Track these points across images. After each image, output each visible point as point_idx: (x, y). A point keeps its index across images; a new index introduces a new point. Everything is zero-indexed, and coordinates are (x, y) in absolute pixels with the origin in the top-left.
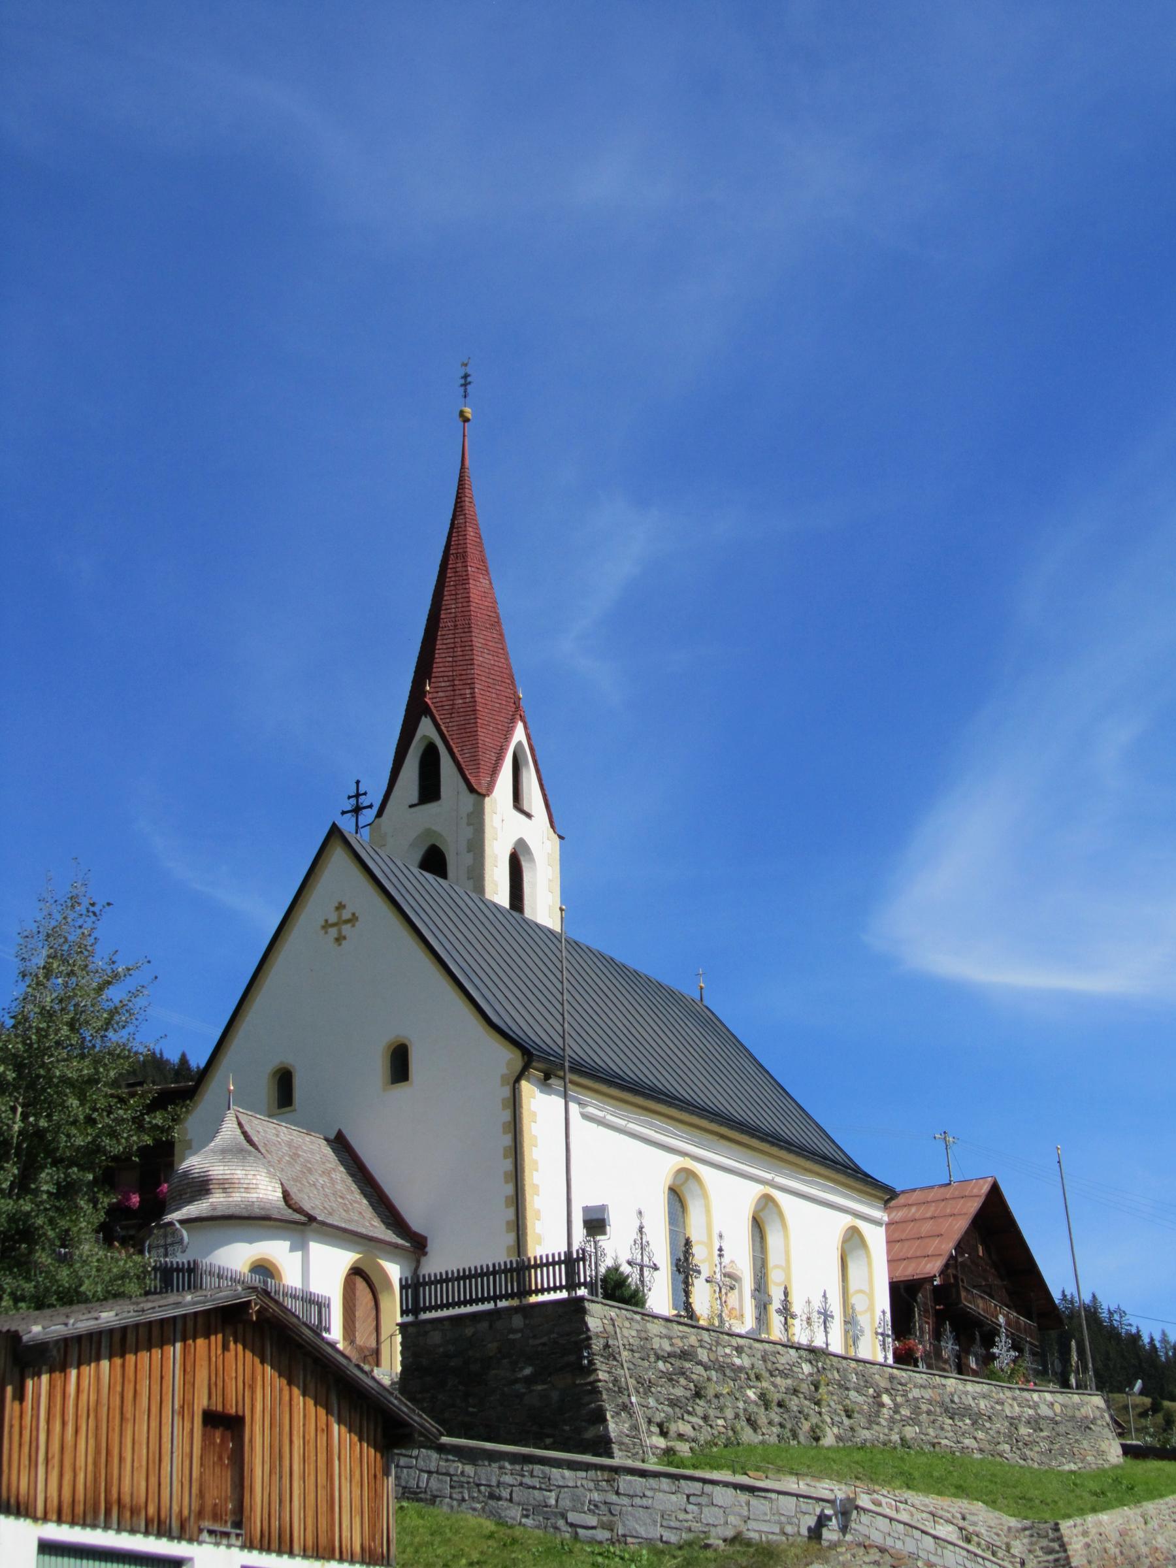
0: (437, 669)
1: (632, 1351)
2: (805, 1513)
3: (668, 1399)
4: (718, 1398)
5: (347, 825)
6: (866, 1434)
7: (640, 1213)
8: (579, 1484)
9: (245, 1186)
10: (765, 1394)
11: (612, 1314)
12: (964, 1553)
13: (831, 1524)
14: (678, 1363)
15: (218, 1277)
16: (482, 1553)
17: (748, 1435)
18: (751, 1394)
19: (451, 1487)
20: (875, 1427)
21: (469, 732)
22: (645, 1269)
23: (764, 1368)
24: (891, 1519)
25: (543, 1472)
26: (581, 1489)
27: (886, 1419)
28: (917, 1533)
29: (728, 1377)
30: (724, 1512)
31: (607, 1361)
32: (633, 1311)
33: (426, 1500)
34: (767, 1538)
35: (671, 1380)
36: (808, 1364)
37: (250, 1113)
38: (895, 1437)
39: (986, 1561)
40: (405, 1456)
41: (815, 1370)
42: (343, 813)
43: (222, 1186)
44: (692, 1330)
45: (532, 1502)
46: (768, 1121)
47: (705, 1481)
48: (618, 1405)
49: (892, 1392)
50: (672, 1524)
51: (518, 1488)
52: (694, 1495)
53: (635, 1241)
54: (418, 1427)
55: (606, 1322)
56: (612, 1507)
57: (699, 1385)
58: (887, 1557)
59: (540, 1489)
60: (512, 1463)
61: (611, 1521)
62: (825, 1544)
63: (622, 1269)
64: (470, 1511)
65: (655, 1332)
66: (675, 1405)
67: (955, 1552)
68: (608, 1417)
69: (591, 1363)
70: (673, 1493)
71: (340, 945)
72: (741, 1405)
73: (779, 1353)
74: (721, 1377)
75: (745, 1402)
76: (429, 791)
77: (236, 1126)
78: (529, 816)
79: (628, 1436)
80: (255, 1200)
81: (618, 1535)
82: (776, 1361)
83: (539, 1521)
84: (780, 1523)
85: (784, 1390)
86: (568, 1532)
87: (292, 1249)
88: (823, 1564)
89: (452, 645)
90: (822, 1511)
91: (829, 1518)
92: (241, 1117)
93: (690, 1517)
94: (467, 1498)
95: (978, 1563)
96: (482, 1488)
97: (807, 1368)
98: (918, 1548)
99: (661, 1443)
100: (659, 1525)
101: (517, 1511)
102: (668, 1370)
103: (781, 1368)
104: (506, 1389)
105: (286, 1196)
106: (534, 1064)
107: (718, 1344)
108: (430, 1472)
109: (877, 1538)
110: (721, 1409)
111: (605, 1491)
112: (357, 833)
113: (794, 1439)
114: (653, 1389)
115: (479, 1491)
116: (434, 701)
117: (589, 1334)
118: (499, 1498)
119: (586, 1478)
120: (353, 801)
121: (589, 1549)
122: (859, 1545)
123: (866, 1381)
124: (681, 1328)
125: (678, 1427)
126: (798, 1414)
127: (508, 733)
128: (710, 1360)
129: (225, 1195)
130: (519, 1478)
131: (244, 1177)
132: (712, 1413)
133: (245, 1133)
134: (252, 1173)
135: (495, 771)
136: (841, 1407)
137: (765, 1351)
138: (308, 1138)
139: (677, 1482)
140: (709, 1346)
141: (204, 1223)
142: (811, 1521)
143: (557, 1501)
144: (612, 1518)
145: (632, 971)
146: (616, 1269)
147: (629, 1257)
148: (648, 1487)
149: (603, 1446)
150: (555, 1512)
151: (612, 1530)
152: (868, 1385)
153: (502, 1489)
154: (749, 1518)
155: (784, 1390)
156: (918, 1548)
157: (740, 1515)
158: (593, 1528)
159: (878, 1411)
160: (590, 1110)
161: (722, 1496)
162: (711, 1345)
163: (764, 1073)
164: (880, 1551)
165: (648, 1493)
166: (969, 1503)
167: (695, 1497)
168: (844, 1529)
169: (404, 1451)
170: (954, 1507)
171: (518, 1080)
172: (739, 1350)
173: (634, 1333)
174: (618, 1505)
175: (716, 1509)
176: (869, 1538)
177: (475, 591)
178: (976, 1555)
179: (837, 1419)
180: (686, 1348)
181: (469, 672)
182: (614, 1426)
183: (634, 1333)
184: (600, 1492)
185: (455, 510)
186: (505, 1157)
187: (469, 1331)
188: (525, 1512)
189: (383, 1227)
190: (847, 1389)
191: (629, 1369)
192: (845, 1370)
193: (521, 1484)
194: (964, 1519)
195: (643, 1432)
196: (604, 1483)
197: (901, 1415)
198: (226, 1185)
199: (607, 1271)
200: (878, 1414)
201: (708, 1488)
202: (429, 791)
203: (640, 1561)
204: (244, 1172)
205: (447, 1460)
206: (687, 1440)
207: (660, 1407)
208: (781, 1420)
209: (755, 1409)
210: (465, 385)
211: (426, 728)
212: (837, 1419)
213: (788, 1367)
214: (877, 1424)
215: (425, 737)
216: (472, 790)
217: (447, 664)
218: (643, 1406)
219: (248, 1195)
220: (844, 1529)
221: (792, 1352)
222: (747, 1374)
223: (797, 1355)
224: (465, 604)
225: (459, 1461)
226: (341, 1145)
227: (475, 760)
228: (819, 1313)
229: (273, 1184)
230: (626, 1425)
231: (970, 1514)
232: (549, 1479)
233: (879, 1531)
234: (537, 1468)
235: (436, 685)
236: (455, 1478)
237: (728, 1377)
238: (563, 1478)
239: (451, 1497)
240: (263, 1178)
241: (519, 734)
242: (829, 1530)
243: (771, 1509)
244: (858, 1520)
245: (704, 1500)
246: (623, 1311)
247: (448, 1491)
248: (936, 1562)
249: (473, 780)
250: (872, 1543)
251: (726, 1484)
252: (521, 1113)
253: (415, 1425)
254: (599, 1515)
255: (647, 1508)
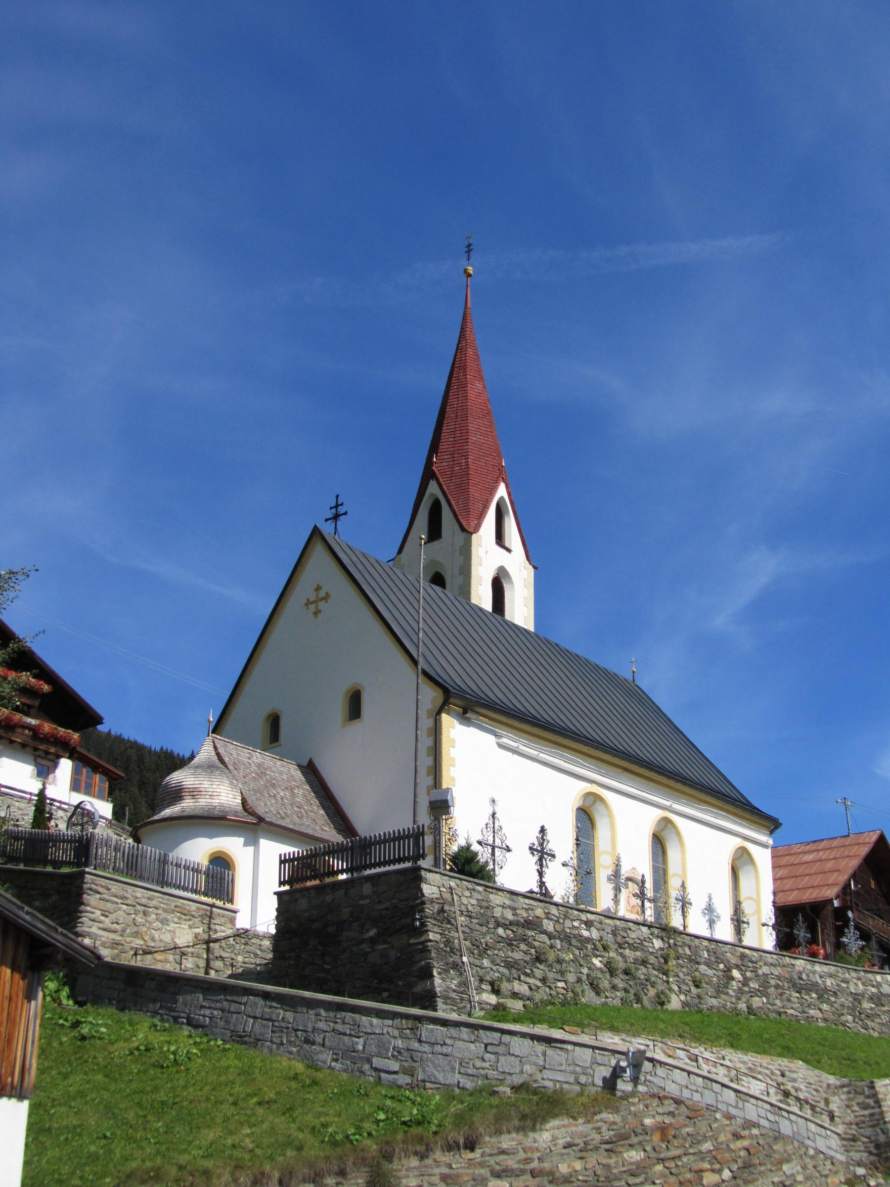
0: (442, 447)
1: (470, 917)
2: (600, 1064)
3: (505, 961)
4: (561, 963)
5: (327, 529)
6: (714, 1002)
7: (494, 801)
8: (385, 1031)
9: (210, 793)
10: (611, 962)
11: (451, 883)
12: (768, 1107)
13: (626, 1075)
14: (520, 931)
15: (184, 868)
16: (278, 1093)
17: (589, 997)
18: (596, 962)
19: (273, 1032)
20: (723, 996)
21: (463, 489)
22: (496, 849)
23: (613, 941)
24: (689, 1073)
25: (354, 1020)
26: (387, 1036)
27: (734, 990)
28: (717, 1087)
29: (574, 946)
30: (520, 1061)
31: (440, 924)
32: (475, 883)
33: (250, 1043)
34: (561, 1086)
35: (510, 945)
36: (660, 940)
37: (227, 740)
38: (742, 1006)
39: (791, 1115)
40: (236, 1002)
41: (667, 945)
42: (327, 520)
43: (191, 794)
44: (539, 904)
45: (342, 1046)
46: (672, 762)
47: (503, 1032)
48: (447, 964)
49: (743, 968)
50: (470, 1071)
51: (330, 1034)
52: (492, 1044)
53: (487, 825)
54: (63, 947)
55: (444, 890)
56: (414, 1053)
57: (539, 950)
58: (683, 1108)
59: (350, 1035)
60: (327, 1010)
61: (412, 1067)
62: (619, 1094)
63: (473, 848)
64: (287, 1054)
65: (497, 902)
66: (512, 967)
67: (757, 1106)
68: (435, 973)
69: (423, 924)
70: (472, 1042)
71: (317, 617)
72: (585, 971)
73: (630, 929)
74: (566, 945)
75: (589, 968)
76: (434, 533)
77: (212, 749)
78: (509, 550)
79: (454, 991)
80: (217, 804)
81: (418, 1081)
82: (626, 935)
83: (347, 1065)
84: (574, 1072)
85: (632, 961)
86: (372, 1076)
87: (246, 844)
88: (612, 1114)
89: (454, 430)
90: (618, 1062)
91: (623, 1070)
92: (216, 741)
93: (486, 1065)
94: (285, 1042)
95: (782, 1116)
96: (299, 1033)
97: (658, 943)
98: (717, 1101)
99: (493, 999)
100: (457, 1072)
101: (328, 1055)
102: (507, 935)
103: (631, 942)
104: (354, 948)
105: (244, 802)
106: (452, 700)
107: (566, 917)
108: (255, 1018)
109: (672, 1089)
110: (562, 973)
111: (409, 1038)
112: (335, 534)
113: (637, 1003)
114: (489, 952)
115: (296, 1036)
116: (439, 468)
117: (424, 899)
118: (313, 1043)
119: (392, 1026)
120: (334, 511)
121: (383, 1092)
122: (653, 1096)
123: (718, 958)
124: (527, 901)
125: (513, 986)
126: (644, 981)
127: (493, 490)
128: (556, 930)
129: (193, 800)
130: (332, 1024)
131: (210, 786)
132: (551, 975)
133: (218, 754)
134: (217, 783)
135: (481, 516)
136: (690, 978)
137: (616, 926)
138: (279, 763)
139: (476, 1032)
140: (556, 919)
141: (174, 822)
142: (606, 1072)
143: (364, 1047)
144: (413, 1064)
145: (584, 660)
146: (468, 848)
147: (480, 838)
148: (449, 1036)
149: (428, 1000)
150: (362, 1057)
151: (413, 1076)
152: (719, 961)
153: (316, 1034)
154: (544, 1068)
155: (632, 961)
156: (717, 1101)
157: (536, 1065)
158: (395, 1073)
159: (728, 983)
160: (504, 740)
161: (519, 1046)
162: (558, 918)
163: (679, 734)
164: (676, 1103)
165: (448, 1041)
166: (789, 1062)
167: (493, 1047)
168: (635, 1080)
169: (235, 998)
170: (773, 1064)
171: (439, 713)
172: (589, 924)
173: (474, 902)
174: (420, 1052)
175: (513, 1058)
176: (665, 1090)
177: (471, 392)
178: (780, 1109)
179: (684, 987)
180: (531, 918)
181: (464, 447)
182: (440, 981)
183: (474, 902)
184: (404, 1040)
185: (460, 338)
186: (428, 775)
187: (329, 898)
188: (335, 1057)
189: (334, 832)
190: (698, 963)
191: (463, 932)
192: (696, 947)
193: (333, 1030)
194: (783, 1075)
195: (472, 989)
196: (408, 1031)
197: (750, 987)
198: (195, 793)
199: (459, 850)
200: (726, 986)
201: (506, 1038)
202: (434, 533)
203: (427, 1106)
204: (210, 783)
205: (271, 1007)
206: (520, 999)
207: (494, 968)
208: (626, 986)
209: (599, 975)
210: (468, 252)
211: (433, 488)
212: (684, 987)
213: (638, 941)
214: (725, 994)
215: (432, 494)
216: (463, 529)
217: (449, 443)
218: (476, 966)
219: (212, 801)
220: (635, 1080)
221: (645, 929)
222: (594, 944)
223: (649, 932)
224: (465, 401)
225: (282, 1008)
226: (311, 772)
227: (467, 510)
228: (677, 899)
229: (234, 793)
230: (455, 982)
231: (790, 1071)
232: (359, 1026)
233: (676, 1083)
234: (349, 1015)
235: (441, 458)
236: (276, 1024)
237: (574, 946)
238: (371, 1025)
239: (271, 1041)
240: (226, 788)
241: (502, 491)
242: (624, 1081)
243: (567, 1060)
244: (653, 1073)
245: (501, 1049)
246: (464, 882)
247: (269, 1035)
248: (736, 1114)
249: (464, 523)
250: (666, 1094)
251: (524, 1035)
252: (441, 739)
253: (59, 945)
254: (401, 1060)
255: (446, 1055)
